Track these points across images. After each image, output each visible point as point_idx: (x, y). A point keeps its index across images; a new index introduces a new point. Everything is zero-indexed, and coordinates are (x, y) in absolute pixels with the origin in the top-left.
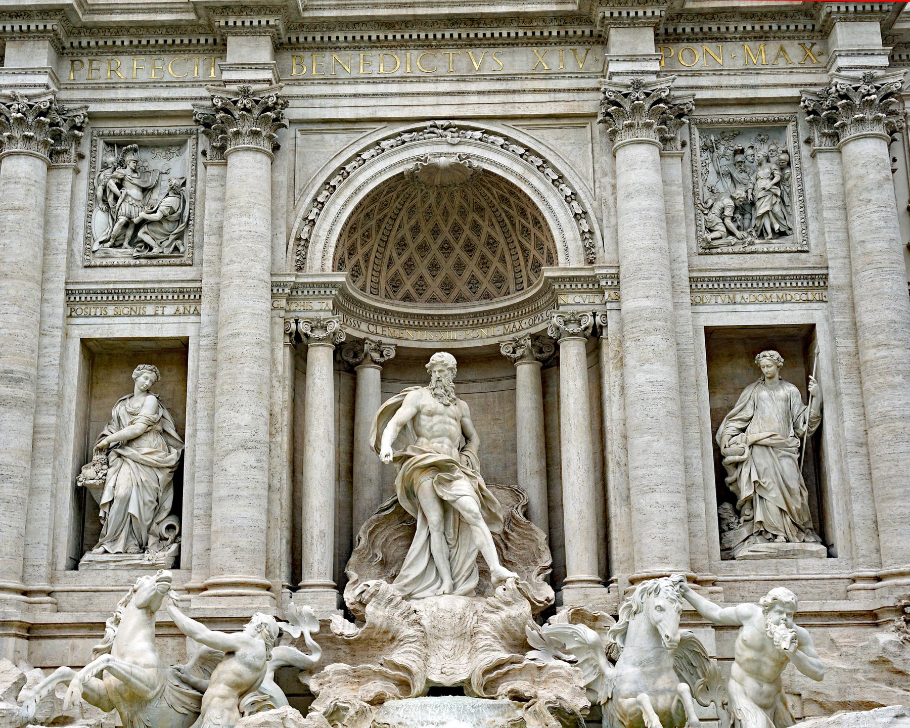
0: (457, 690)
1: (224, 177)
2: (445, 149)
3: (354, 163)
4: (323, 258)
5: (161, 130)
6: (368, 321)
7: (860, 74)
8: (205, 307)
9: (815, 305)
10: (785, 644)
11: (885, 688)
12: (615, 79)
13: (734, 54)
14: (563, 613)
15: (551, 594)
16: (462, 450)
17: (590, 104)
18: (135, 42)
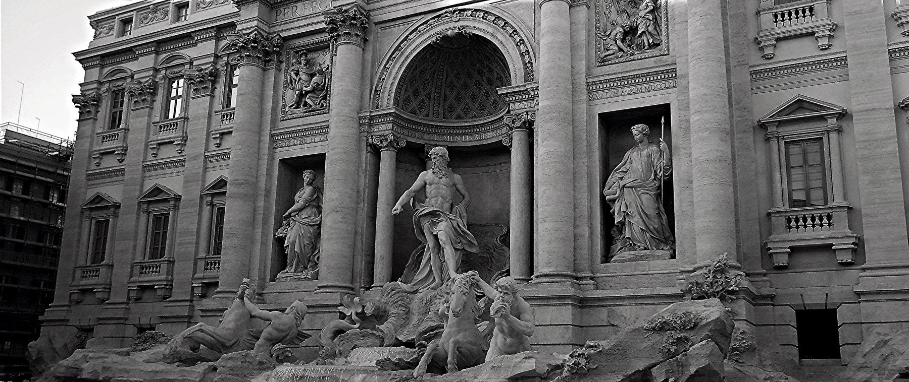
2: (452, 25)
4: (389, 100)
9: (670, 90)
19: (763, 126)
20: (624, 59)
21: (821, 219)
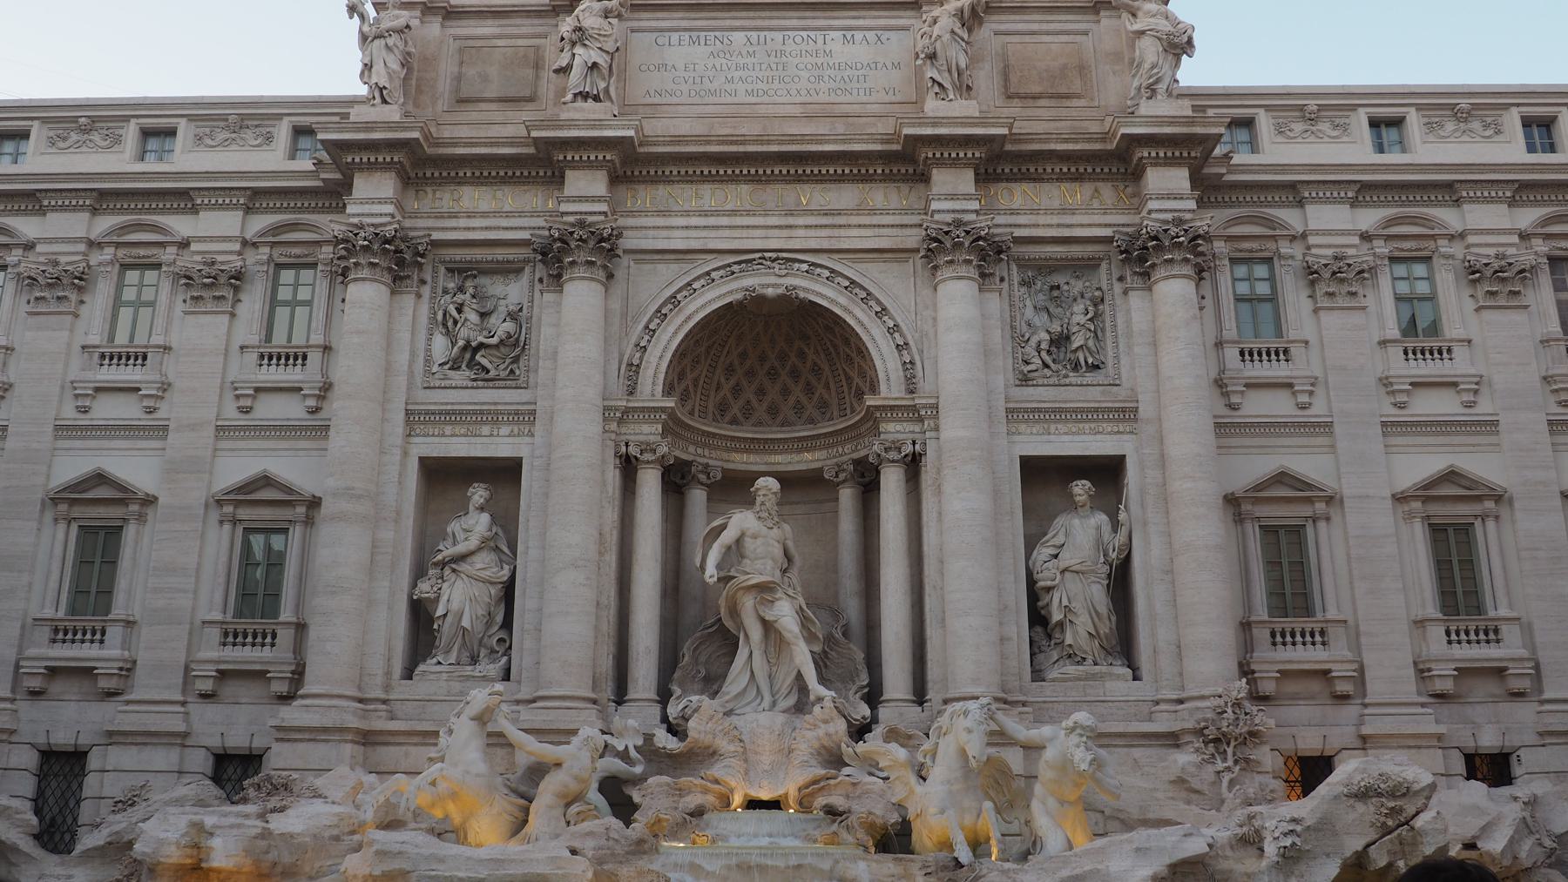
0: (774, 805)
1: (559, 304)
2: (773, 280)
3: (685, 293)
4: (654, 384)
5: (500, 258)
6: (696, 444)
7: (1169, 216)
8: (539, 428)
9: (1125, 437)
10: (1084, 766)
11: (1183, 806)
12: (937, 217)
13: (1051, 195)
14: (878, 730)
15: (868, 712)
16: (784, 571)
17: (912, 239)
18: (477, 174)
19: (1231, 501)
20: (1054, 380)
21: (1312, 635)
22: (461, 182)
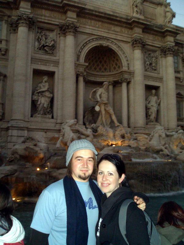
2: (104, 43)
8: (60, 66)
12: (136, 37)
17: (129, 40)
22: (42, 8)
